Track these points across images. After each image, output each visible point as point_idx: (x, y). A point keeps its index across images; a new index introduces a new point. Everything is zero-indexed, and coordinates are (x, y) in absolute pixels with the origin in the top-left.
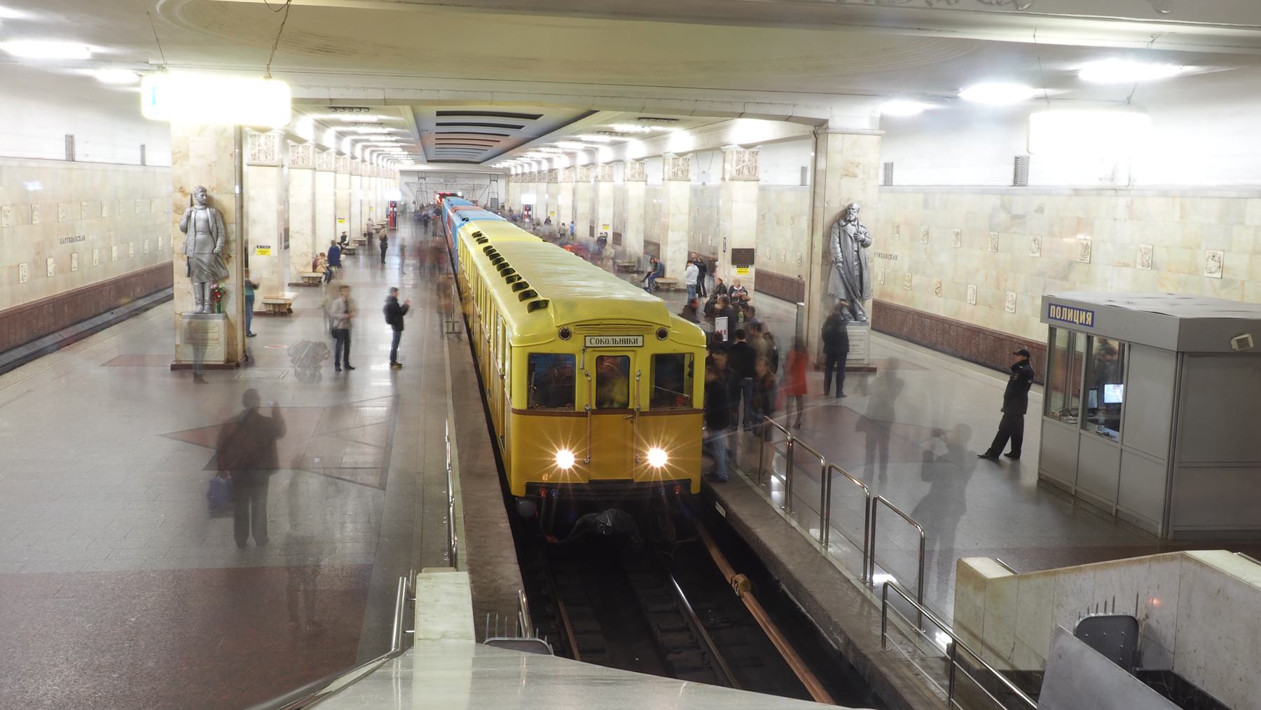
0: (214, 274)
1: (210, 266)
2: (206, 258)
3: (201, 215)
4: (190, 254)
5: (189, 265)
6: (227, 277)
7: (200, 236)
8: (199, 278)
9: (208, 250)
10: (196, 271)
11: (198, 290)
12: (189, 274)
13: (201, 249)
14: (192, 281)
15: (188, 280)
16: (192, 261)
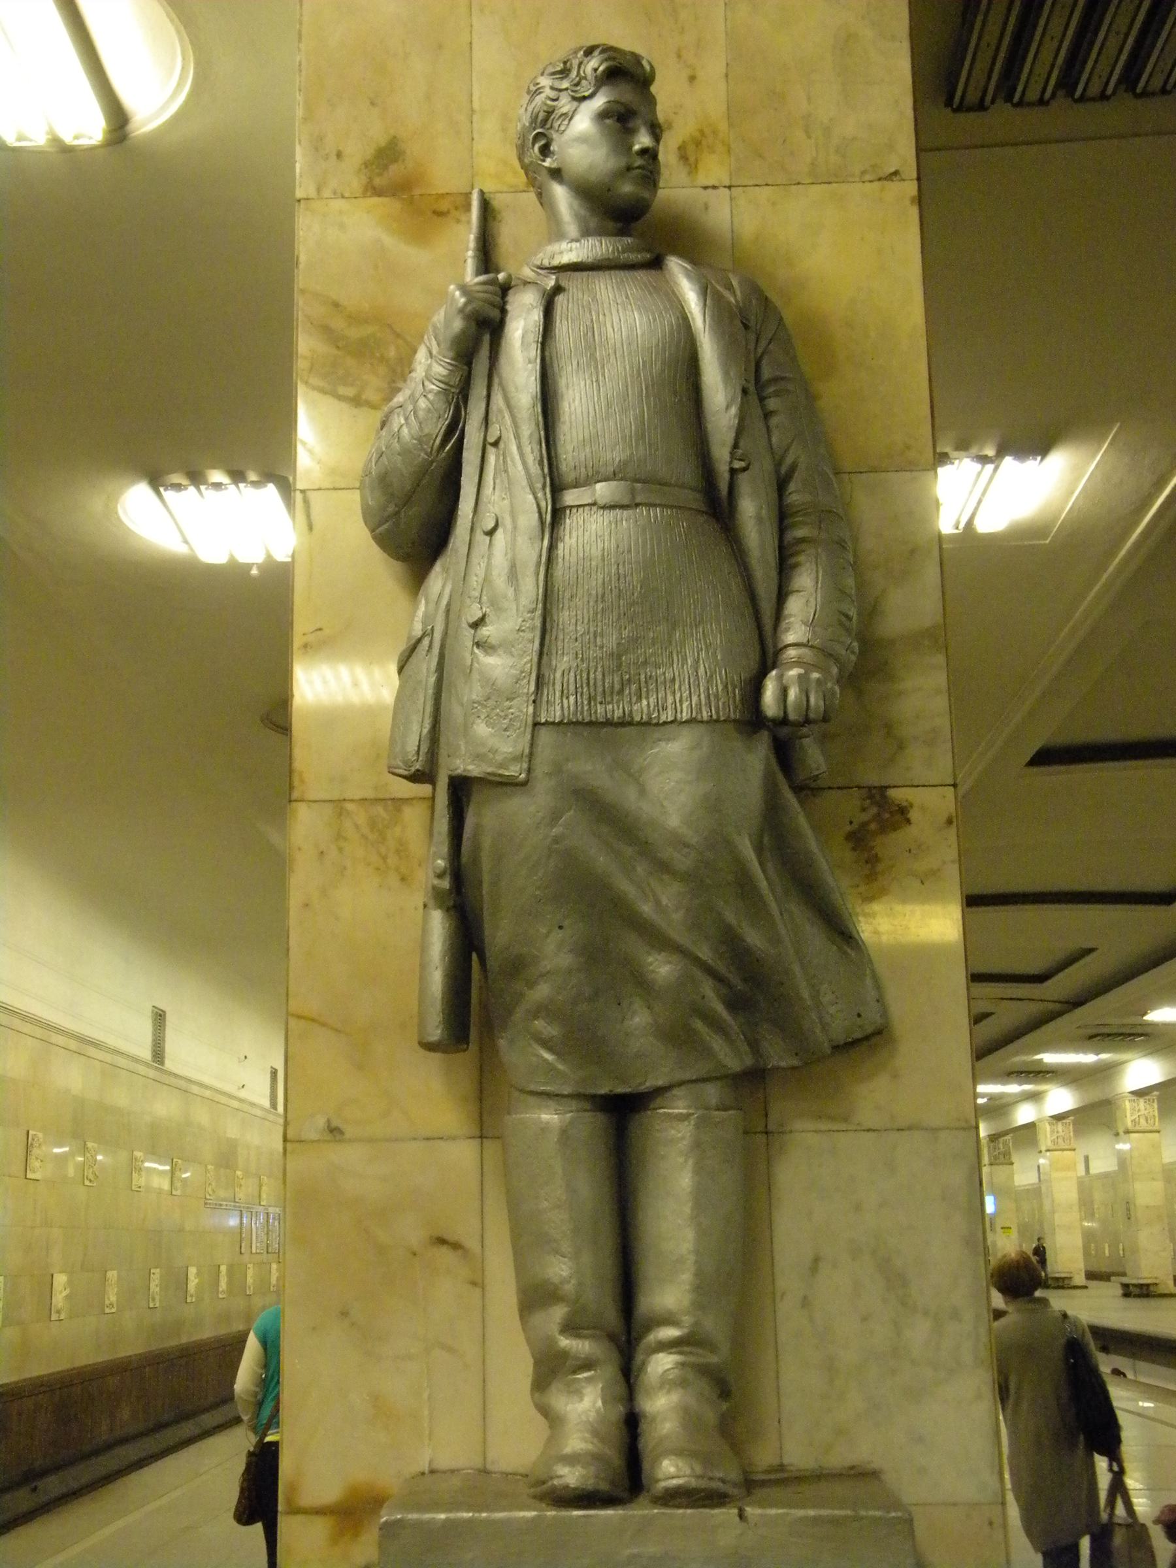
0: (751, 989)
1: (712, 875)
2: (672, 782)
3: (610, 340)
4: (488, 741)
5: (462, 900)
6: (869, 1042)
7: (592, 533)
8: (584, 1041)
9: (691, 678)
10: (555, 951)
11: (565, 1190)
12: (471, 1012)
13: (625, 669)
14: (488, 1104)
15: (429, 1093)
16: (518, 827)
